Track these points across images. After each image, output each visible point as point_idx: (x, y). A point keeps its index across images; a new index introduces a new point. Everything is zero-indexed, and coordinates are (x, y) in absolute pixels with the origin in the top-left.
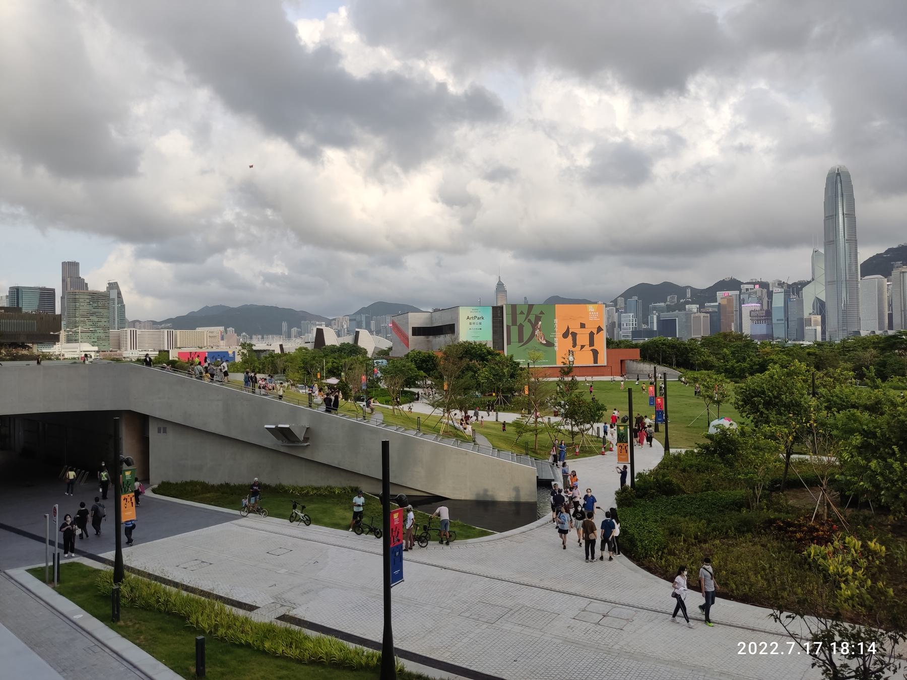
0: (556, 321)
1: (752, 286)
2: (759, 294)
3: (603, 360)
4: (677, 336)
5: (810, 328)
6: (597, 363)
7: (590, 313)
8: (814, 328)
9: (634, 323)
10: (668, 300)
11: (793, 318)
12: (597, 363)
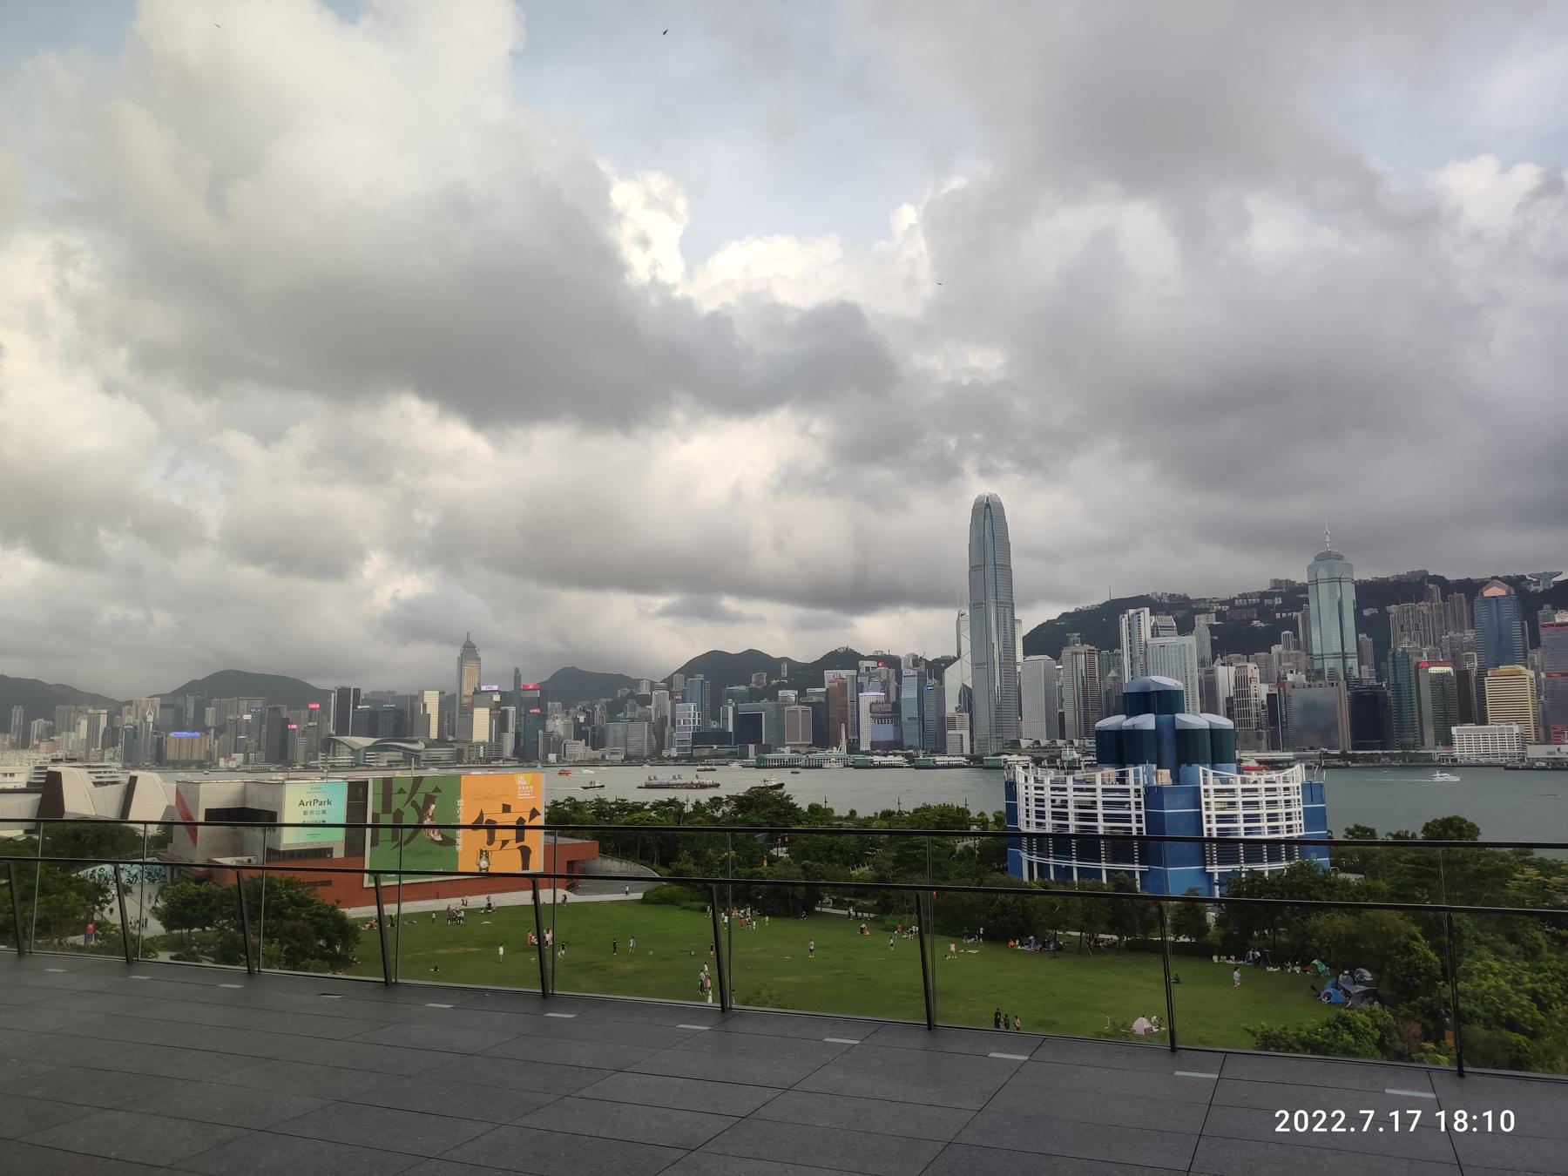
0: (461, 802)
1: (873, 664)
2: (884, 677)
3: (537, 865)
4: (764, 743)
5: (954, 732)
6: (528, 869)
7: (520, 788)
8: (958, 732)
9: (697, 719)
10: (753, 681)
11: (930, 716)
12: (528, 869)
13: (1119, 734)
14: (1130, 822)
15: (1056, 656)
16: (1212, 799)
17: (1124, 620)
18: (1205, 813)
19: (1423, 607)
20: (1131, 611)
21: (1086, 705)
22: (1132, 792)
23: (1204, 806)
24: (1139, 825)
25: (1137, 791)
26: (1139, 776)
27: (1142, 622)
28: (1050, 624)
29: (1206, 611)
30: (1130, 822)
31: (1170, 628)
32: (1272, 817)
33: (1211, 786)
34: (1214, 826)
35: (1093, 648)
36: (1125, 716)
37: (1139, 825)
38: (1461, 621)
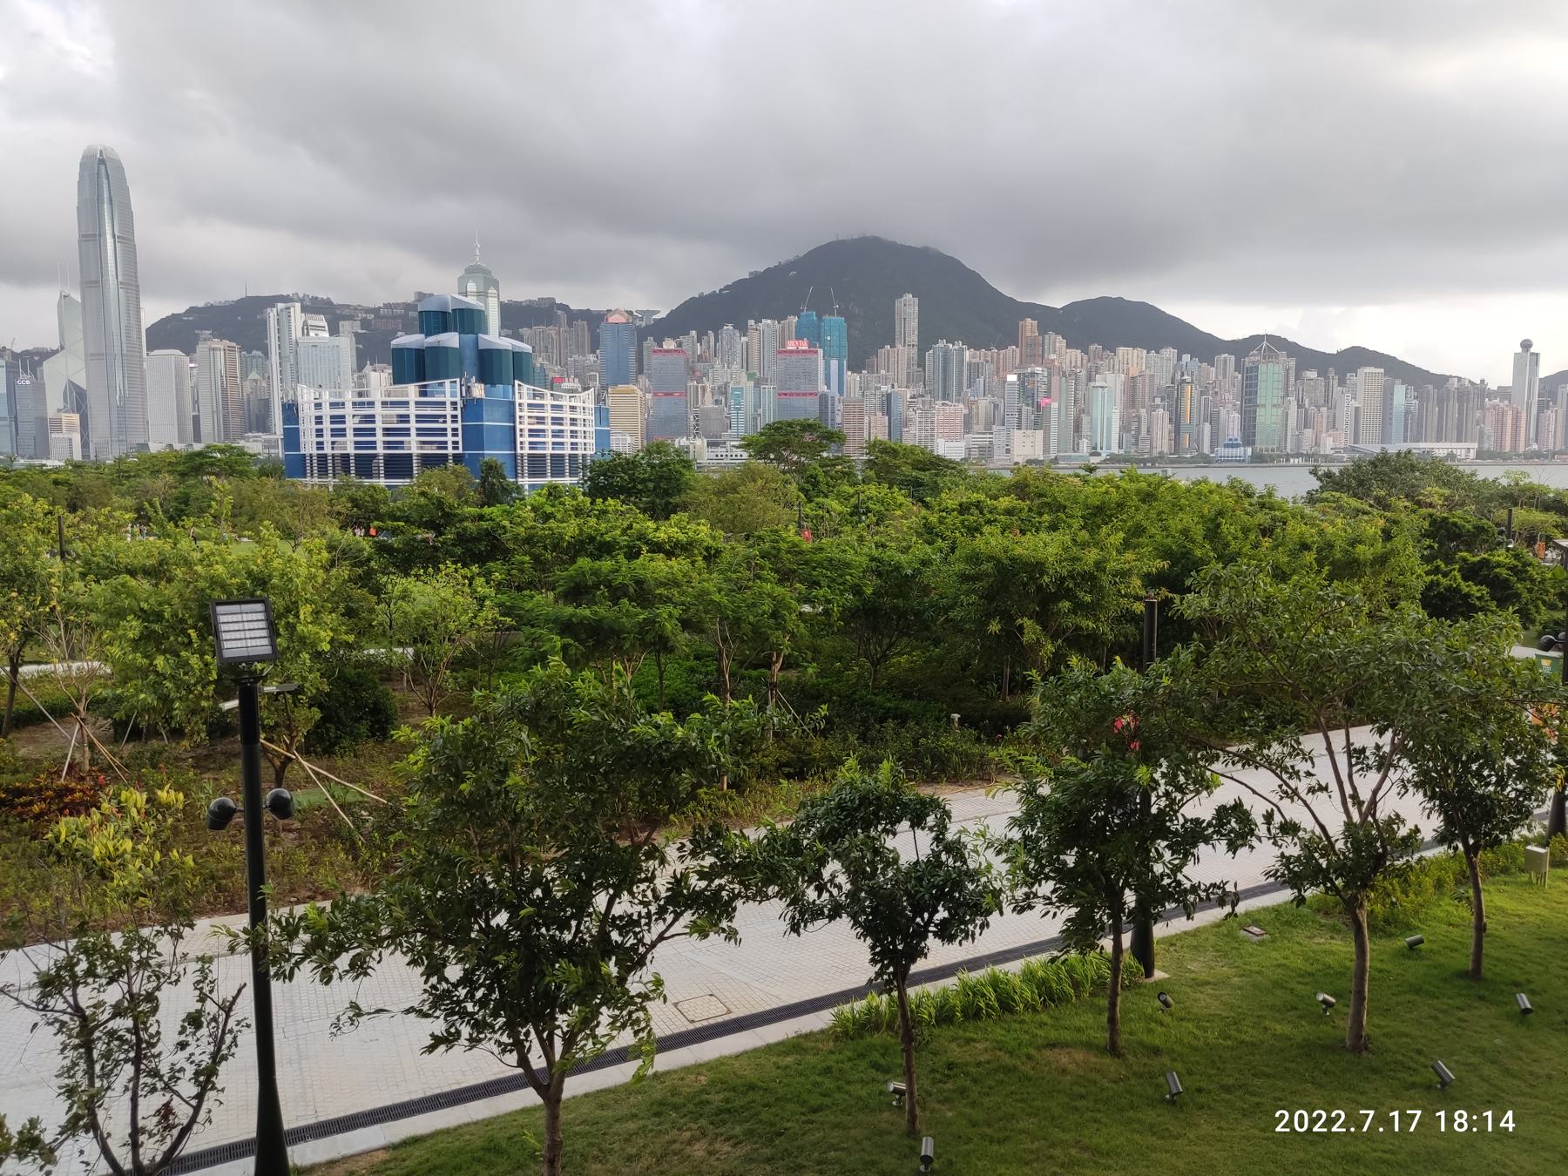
13: (420, 354)
14: (446, 435)
15: (189, 350)
16: (526, 413)
17: (272, 314)
18: (518, 427)
19: (552, 331)
20: (280, 306)
21: (225, 407)
22: (448, 405)
23: (518, 420)
24: (455, 439)
25: (454, 404)
26: (449, 391)
27: (292, 318)
28: (174, 317)
29: (351, 318)
30: (446, 435)
31: (321, 328)
32: (574, 434)
33: (526, 401)
34: (527, 439)
35: (234, 344)
36: (423, 336)
37: (455, 439)
38: (583, 346)
